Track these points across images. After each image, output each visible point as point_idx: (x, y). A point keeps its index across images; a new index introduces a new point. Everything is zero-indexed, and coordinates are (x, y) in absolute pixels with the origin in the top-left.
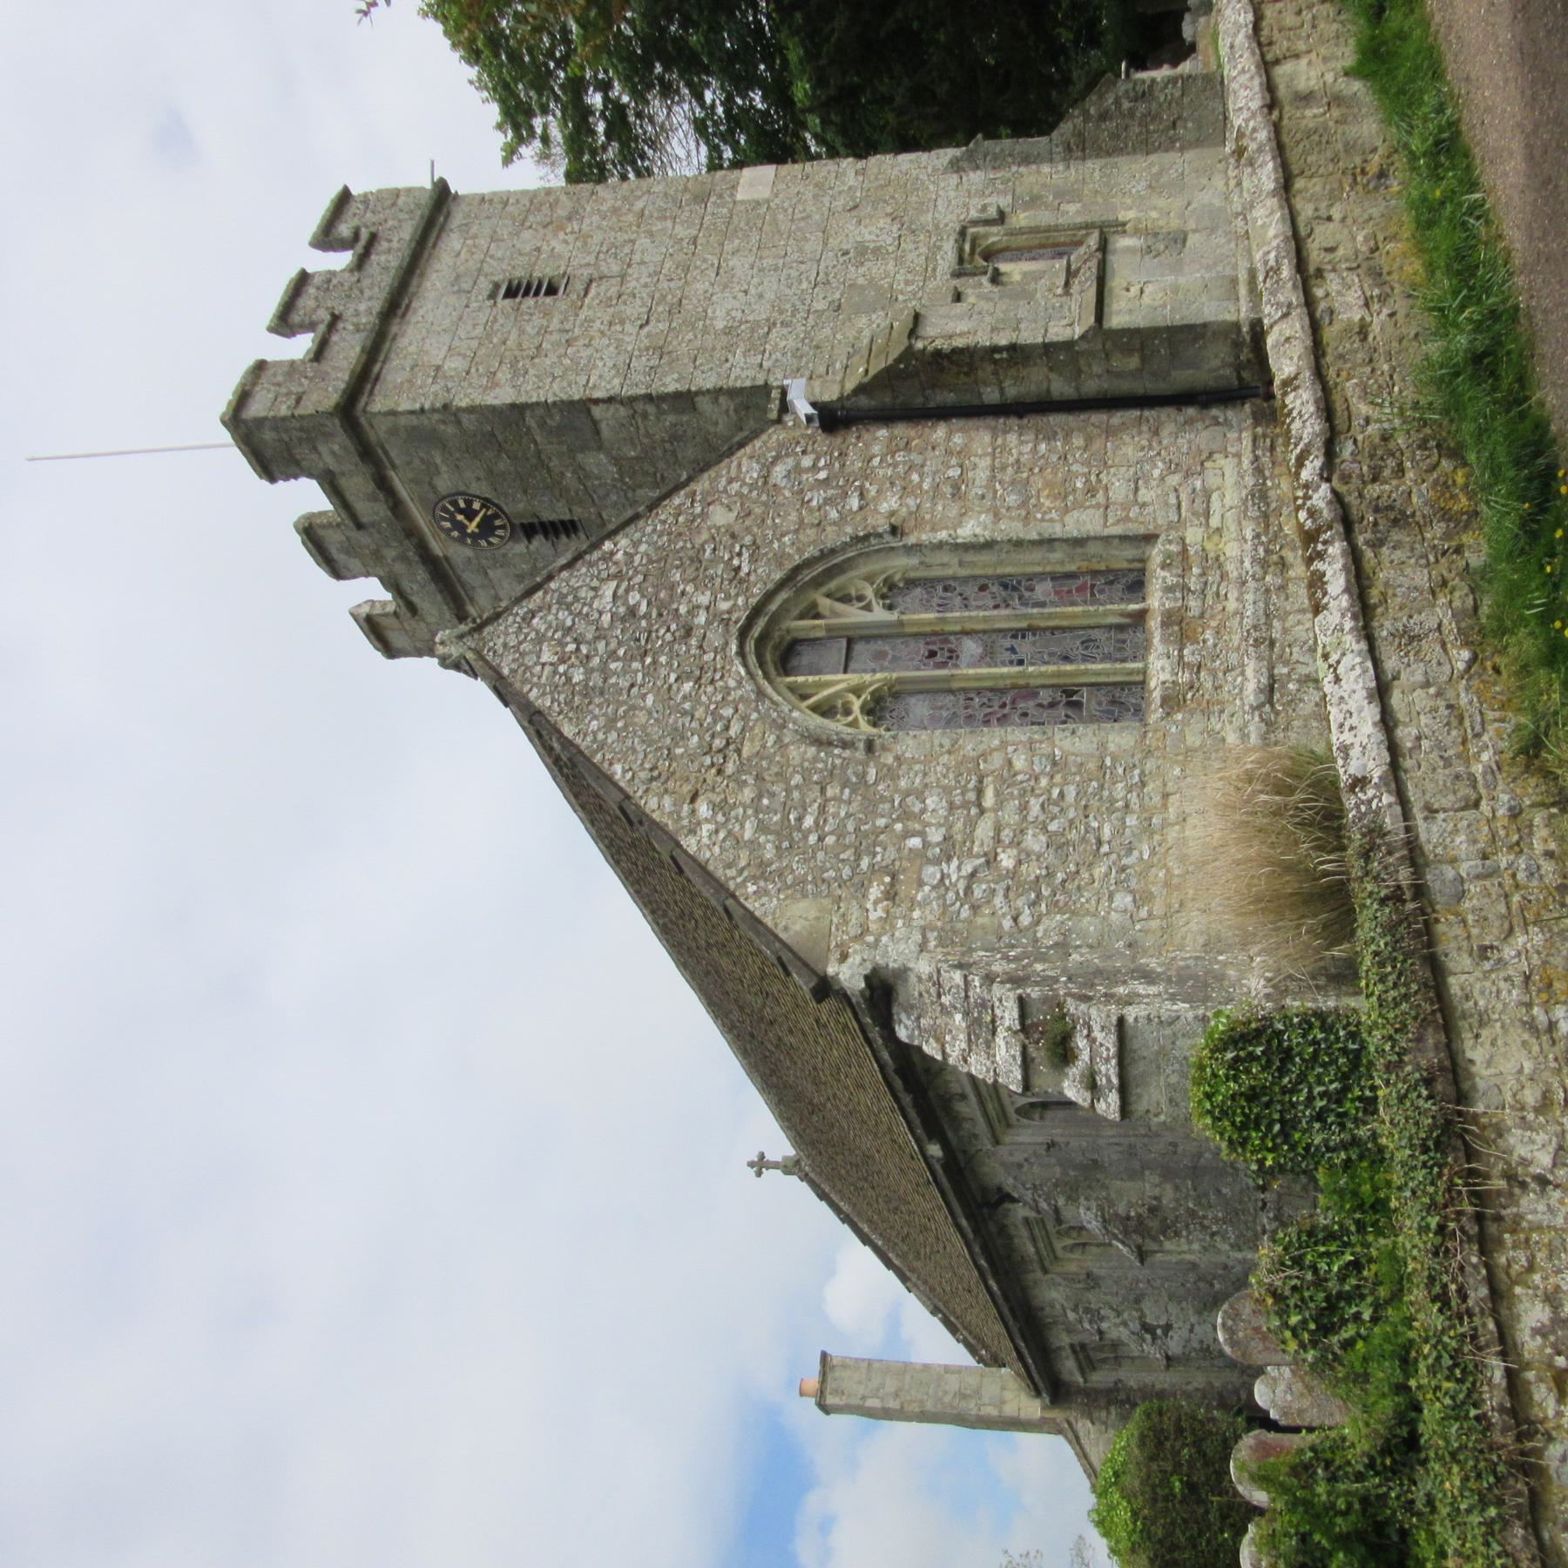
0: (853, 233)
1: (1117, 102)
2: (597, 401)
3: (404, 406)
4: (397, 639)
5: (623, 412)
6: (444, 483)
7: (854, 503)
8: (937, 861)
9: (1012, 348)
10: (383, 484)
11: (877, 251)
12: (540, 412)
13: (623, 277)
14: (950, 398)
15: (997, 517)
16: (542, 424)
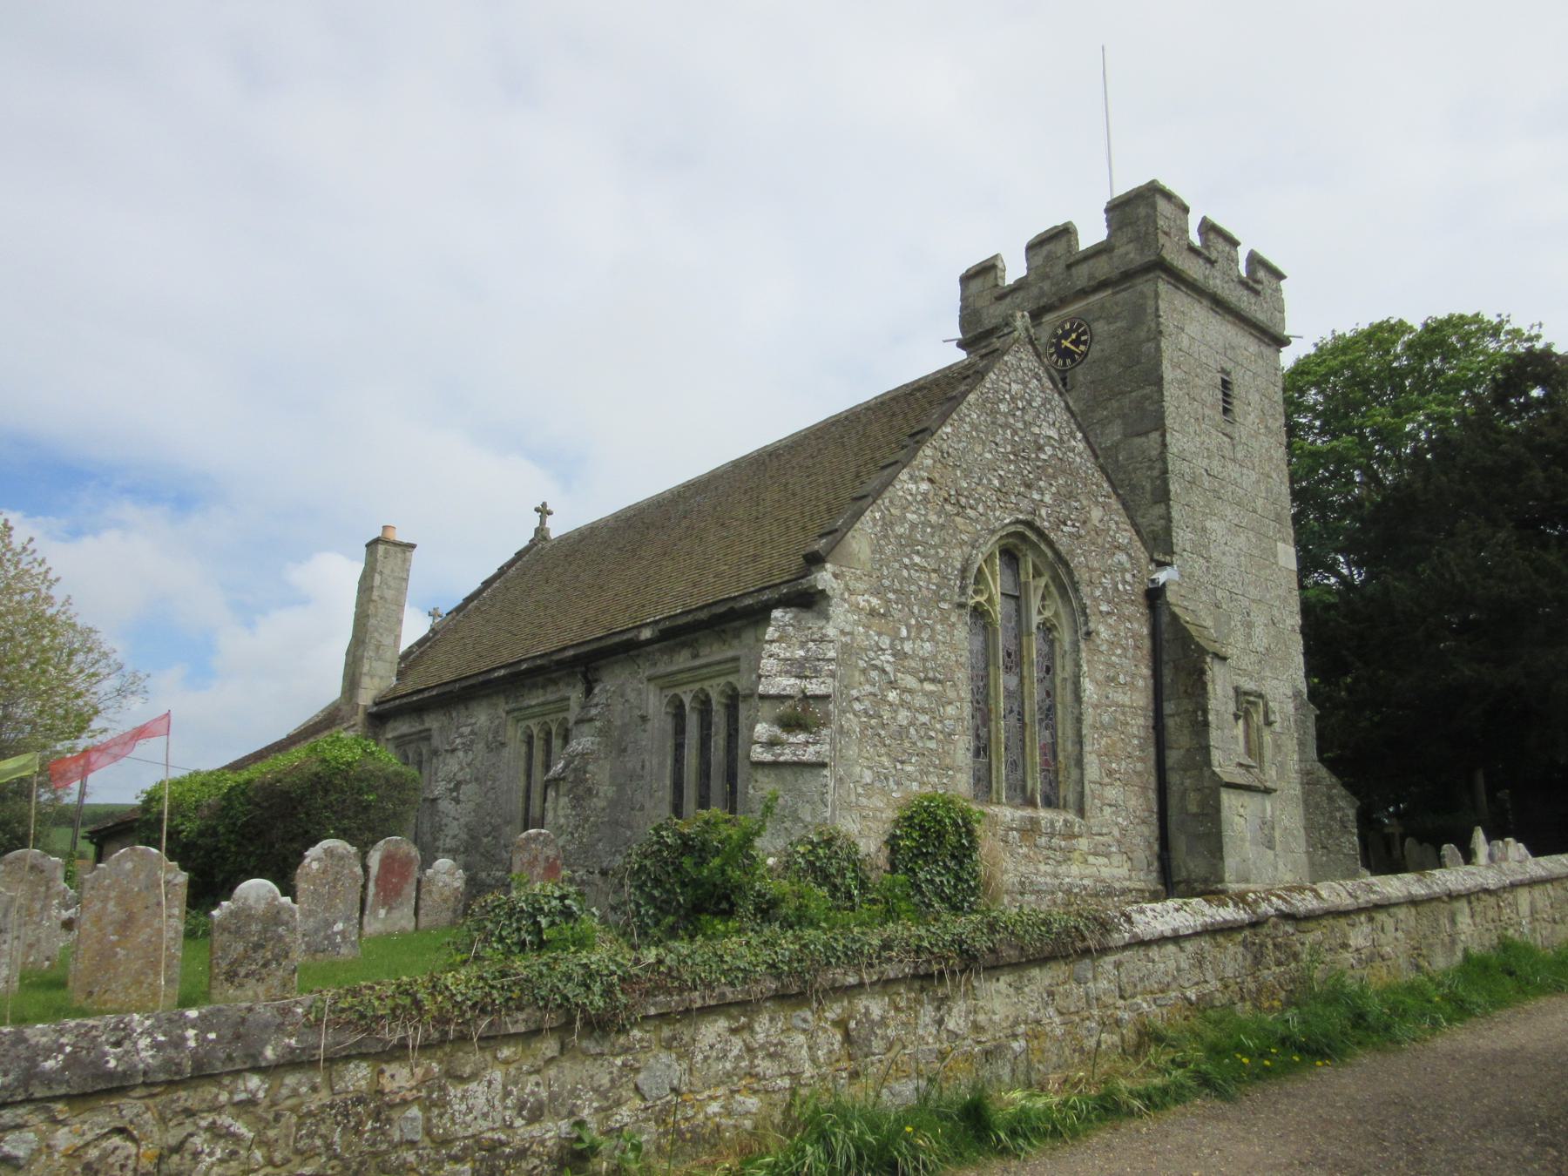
0: (1260, 620)
1: (1340, 809)
2: (1163, 436)
3: (1162, 305)
5: (1154, 453)
6: (1100, 327)
7: (1104, 608)
8: (892, 646)
9: (1206, 724)
10: (1103, 285)
11: (1249, 636)
12: (1156, 397)
13: (1234, 460)
14: (1167, 680)
15: (1096, 707)
16: (1145, 397)
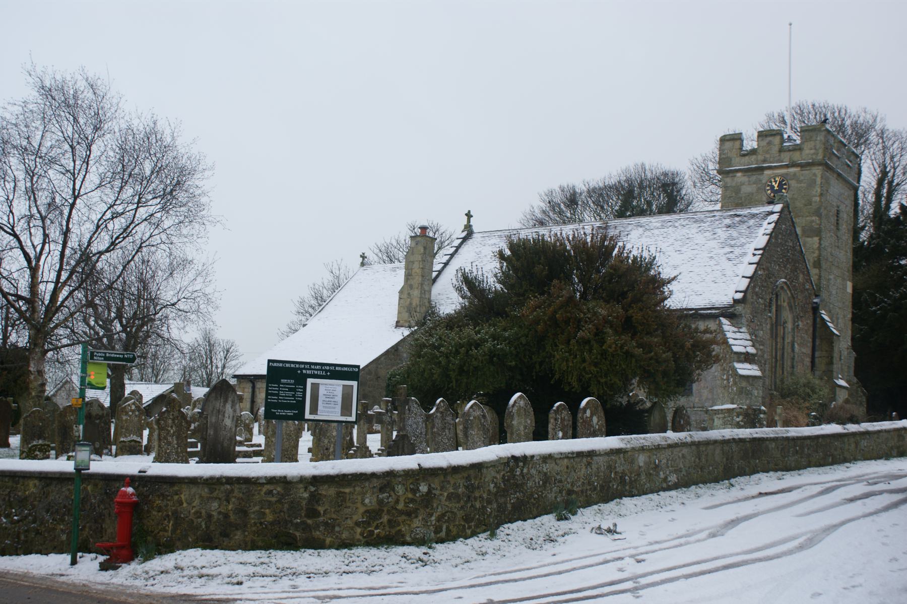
4: (728, 145)
6: (793, 183)
14: (817, 343)
16: (813, 221)
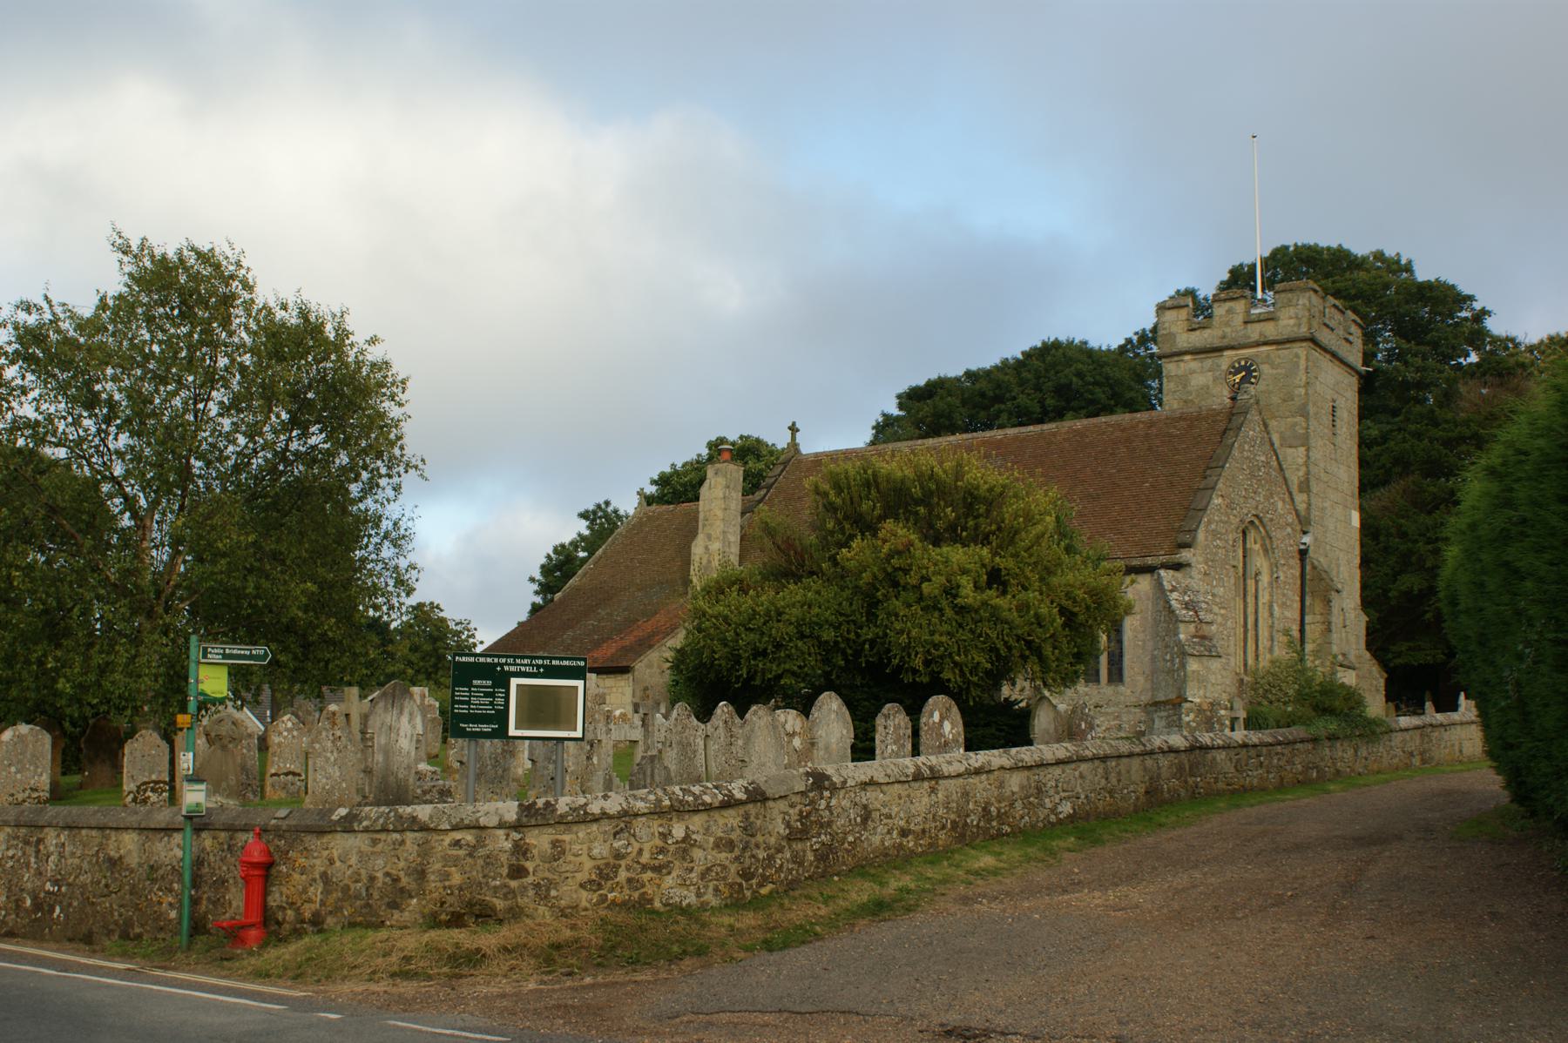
5: (1301, 461)
6: (1265, 368)
16: (1296, 424)
